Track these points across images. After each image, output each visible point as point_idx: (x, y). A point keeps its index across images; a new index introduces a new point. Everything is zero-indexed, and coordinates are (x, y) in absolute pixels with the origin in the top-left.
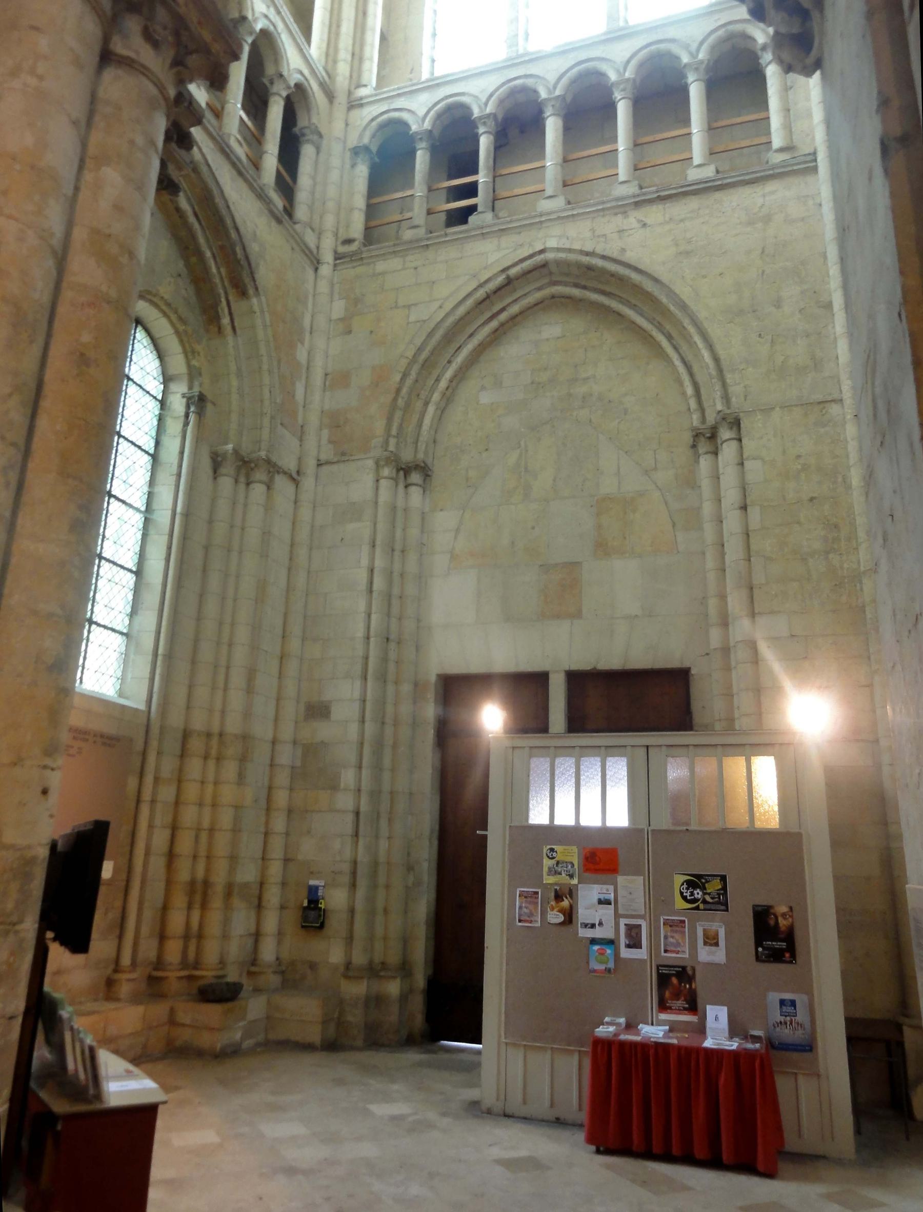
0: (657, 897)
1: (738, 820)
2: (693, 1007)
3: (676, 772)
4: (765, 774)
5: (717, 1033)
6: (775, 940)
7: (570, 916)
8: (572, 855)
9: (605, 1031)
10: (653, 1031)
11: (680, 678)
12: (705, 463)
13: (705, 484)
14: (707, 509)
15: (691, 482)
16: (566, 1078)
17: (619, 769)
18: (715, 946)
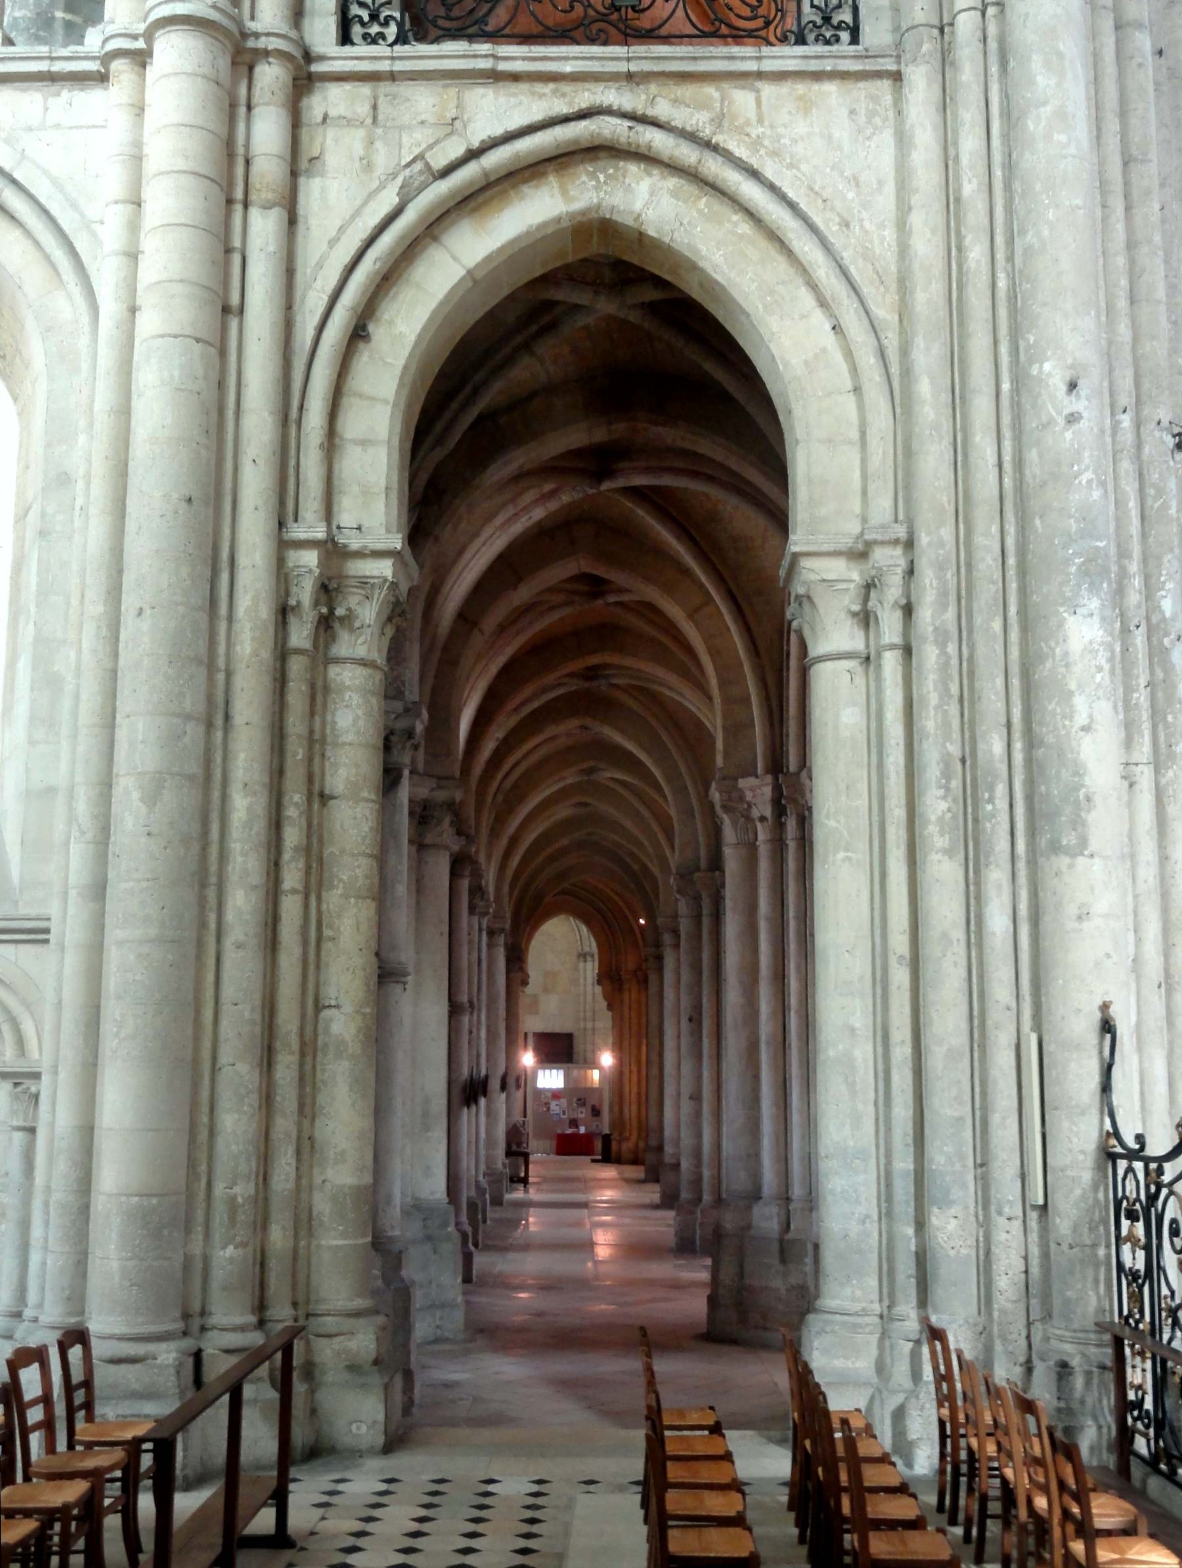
0: (569, 1104)
1: (589, 1085)
2: (577, 1127)
3: (575, 1073)
4: (595, 1075)
5: (582, 1130)
6: (596, 1112)
7: (548, 1109)
8: (549, 1095)
9: (559, 1132)
10: (569, 1131)
11: (569, 1037)
12: (581, 965)
13: (582, 973)
14: (582, 981)
15: (576, 969)
16: (551, 1144)
17: (561, 1073)
18: (582, 1114)
